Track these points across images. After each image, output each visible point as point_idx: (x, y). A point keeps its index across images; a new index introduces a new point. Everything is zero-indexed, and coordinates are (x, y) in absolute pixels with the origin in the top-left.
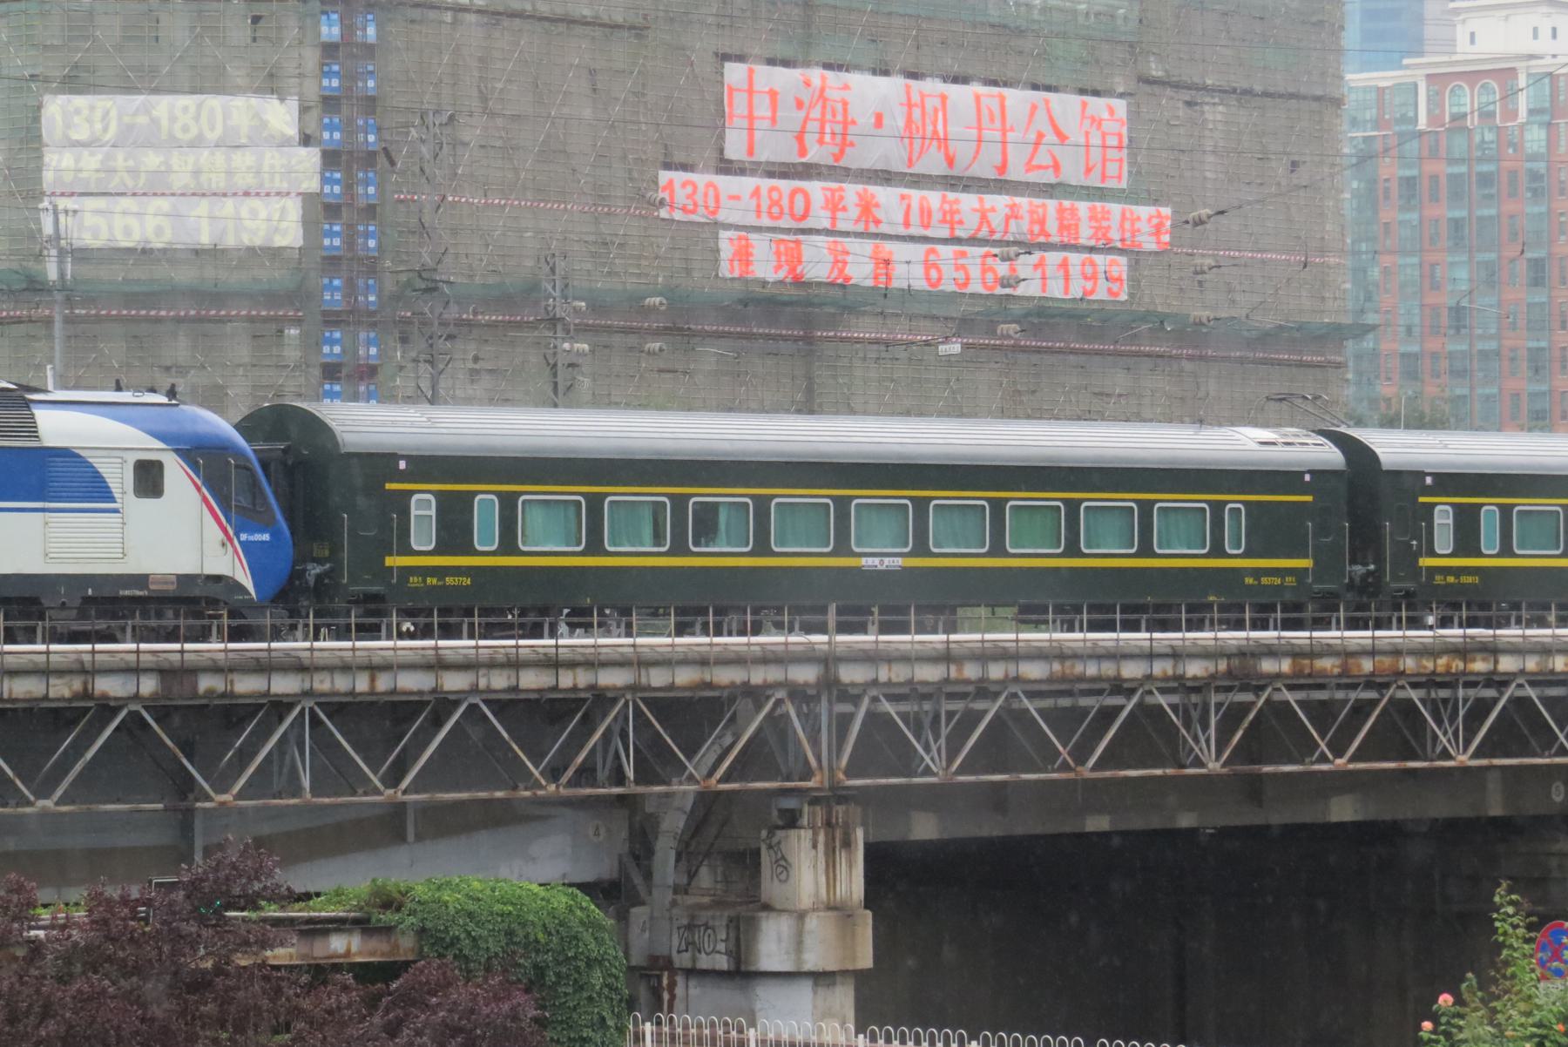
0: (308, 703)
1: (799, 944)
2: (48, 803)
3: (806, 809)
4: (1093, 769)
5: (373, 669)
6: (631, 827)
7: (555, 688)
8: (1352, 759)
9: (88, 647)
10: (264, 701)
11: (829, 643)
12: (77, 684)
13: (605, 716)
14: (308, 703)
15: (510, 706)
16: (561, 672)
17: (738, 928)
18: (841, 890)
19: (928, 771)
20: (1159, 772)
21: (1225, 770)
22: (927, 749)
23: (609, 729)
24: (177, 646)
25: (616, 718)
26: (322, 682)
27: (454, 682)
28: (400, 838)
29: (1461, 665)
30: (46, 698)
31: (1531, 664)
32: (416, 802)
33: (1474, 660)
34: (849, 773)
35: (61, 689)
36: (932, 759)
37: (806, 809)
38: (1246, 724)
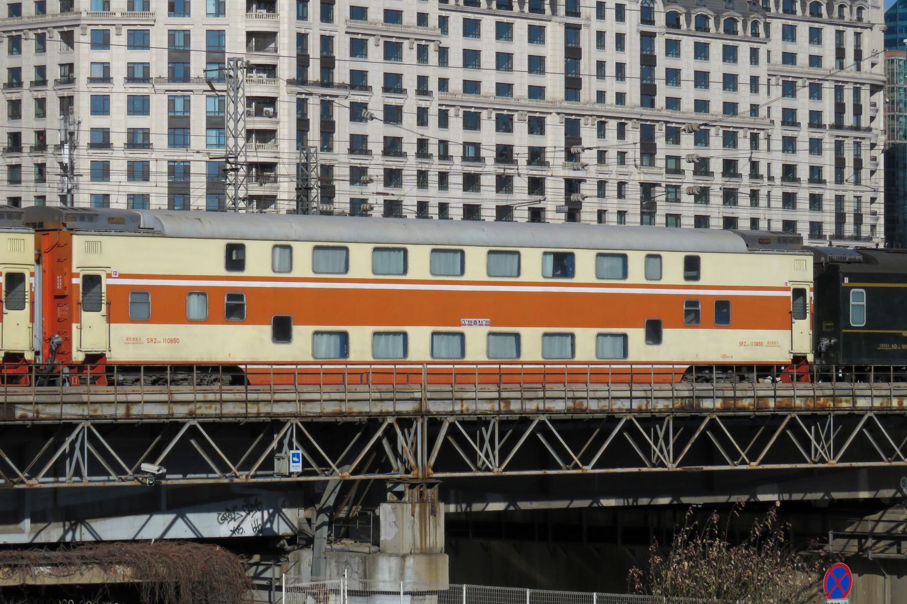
1: (402, 575)
3: (407, 491)
4: (593, 468)
5: (128, 403)
7: (246, 416)
8: (762, 463)
15: (217, 428)
16: (249, 405)
17: (365, 566)
18: (430, 542)
19: (488, 469)
20: (635, 470)
21: (678, 469)
22: (487, 456)
26: (95, 411)
27: (180, 411)
29: (832, 404)
31: (877, 403)
33: (841, 401)
34: (436, 469)
36: (490, 463)
37: (407, 491)
38: (693, 440)
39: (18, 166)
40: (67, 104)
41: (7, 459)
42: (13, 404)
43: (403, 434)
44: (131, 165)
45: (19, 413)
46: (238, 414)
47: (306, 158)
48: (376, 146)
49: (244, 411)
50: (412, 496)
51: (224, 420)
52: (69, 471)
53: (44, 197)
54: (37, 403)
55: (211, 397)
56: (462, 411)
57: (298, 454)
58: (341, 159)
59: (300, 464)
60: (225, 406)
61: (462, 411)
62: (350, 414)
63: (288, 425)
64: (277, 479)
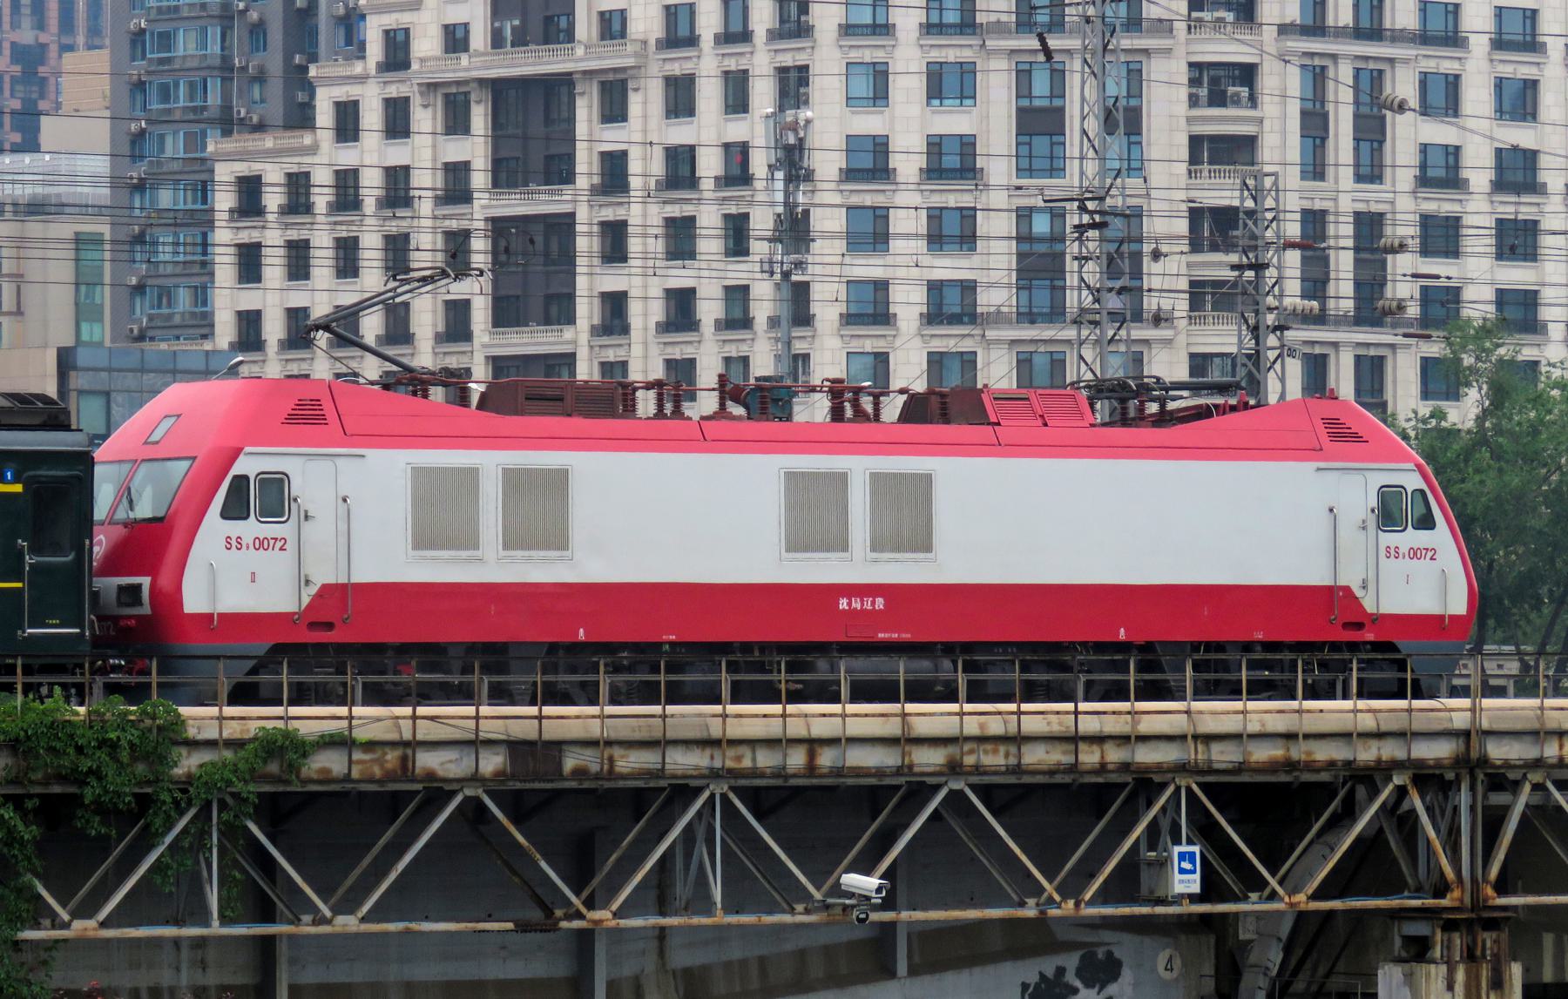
0: (720, 788)
2: (348, 923)
6: (1217, 957)
7: (1073, 768)
9: (407, 711)
10: (663, 783)
11: (1473, 710)
12: (392, 757)
13: (1149, 804)
14: (720, 788)
15: (1015, 796)
16: (1082, 746)
23: (1155, 821)
24: (533, 710)
25: (1164, 809)
26: (739, 759)
27: (929, 759)
28: (889, 972)
30: (347, 778)
32: (910, 923)
34: (1502, 887)
35: (362, 766)
39: (691, 220)
40: (793, 85)
41: (543, 864)
42: (558, 746)
43: (1428, 809)
44: (936, 216)
45: (570, 763)
46: (1059, 764)
47: (1255, 199)
48: (1478, 171)
49: (1068, 759)
50: (1448, 946)
51: (1027, 779)
52: (682, 890)
53: (745, 289)
54: (609, 743)
55: (995, 727)
56: (1561, 759)
57: (1192, 854)
58: (1403, 203)
59: (1197, 876)
60: (1024, 749)
61: (1561, 759)
62: (1310, 766)
63: (1171, 789)
64: (1145, 910)
